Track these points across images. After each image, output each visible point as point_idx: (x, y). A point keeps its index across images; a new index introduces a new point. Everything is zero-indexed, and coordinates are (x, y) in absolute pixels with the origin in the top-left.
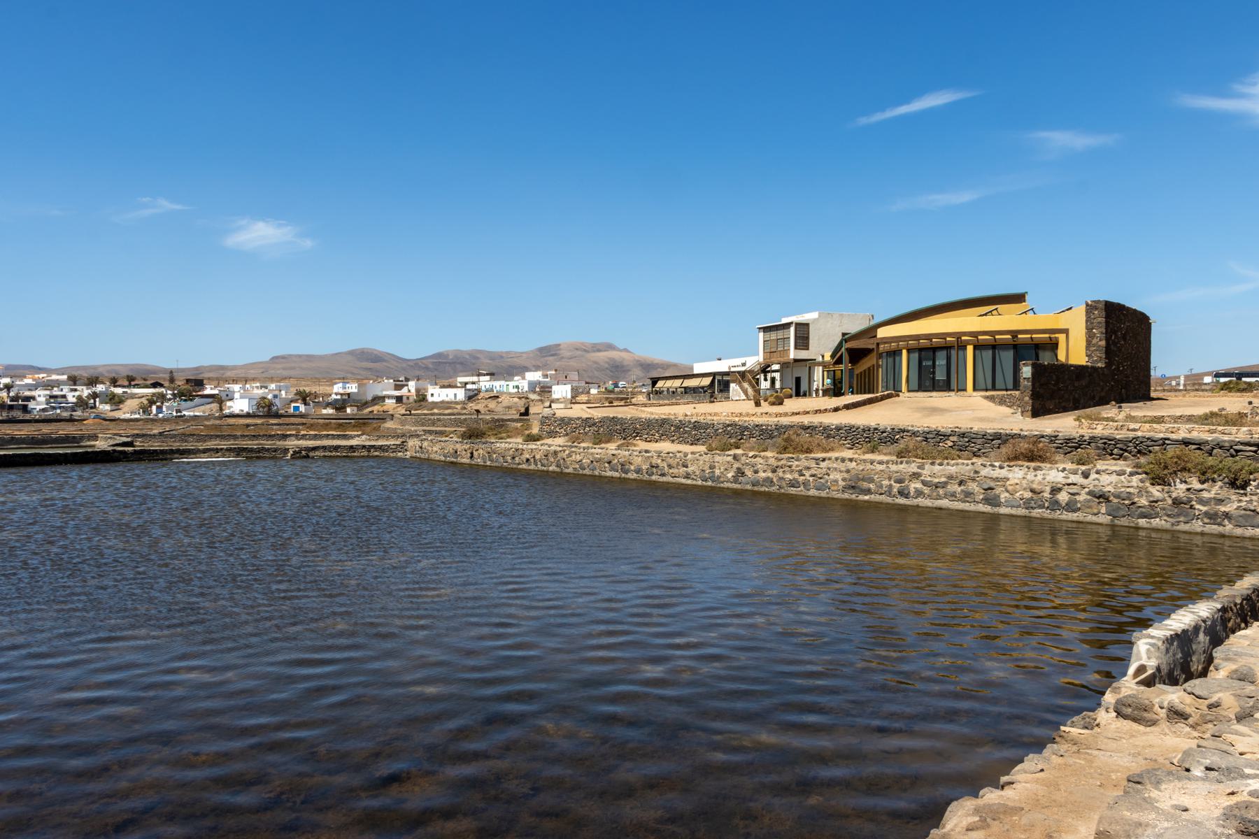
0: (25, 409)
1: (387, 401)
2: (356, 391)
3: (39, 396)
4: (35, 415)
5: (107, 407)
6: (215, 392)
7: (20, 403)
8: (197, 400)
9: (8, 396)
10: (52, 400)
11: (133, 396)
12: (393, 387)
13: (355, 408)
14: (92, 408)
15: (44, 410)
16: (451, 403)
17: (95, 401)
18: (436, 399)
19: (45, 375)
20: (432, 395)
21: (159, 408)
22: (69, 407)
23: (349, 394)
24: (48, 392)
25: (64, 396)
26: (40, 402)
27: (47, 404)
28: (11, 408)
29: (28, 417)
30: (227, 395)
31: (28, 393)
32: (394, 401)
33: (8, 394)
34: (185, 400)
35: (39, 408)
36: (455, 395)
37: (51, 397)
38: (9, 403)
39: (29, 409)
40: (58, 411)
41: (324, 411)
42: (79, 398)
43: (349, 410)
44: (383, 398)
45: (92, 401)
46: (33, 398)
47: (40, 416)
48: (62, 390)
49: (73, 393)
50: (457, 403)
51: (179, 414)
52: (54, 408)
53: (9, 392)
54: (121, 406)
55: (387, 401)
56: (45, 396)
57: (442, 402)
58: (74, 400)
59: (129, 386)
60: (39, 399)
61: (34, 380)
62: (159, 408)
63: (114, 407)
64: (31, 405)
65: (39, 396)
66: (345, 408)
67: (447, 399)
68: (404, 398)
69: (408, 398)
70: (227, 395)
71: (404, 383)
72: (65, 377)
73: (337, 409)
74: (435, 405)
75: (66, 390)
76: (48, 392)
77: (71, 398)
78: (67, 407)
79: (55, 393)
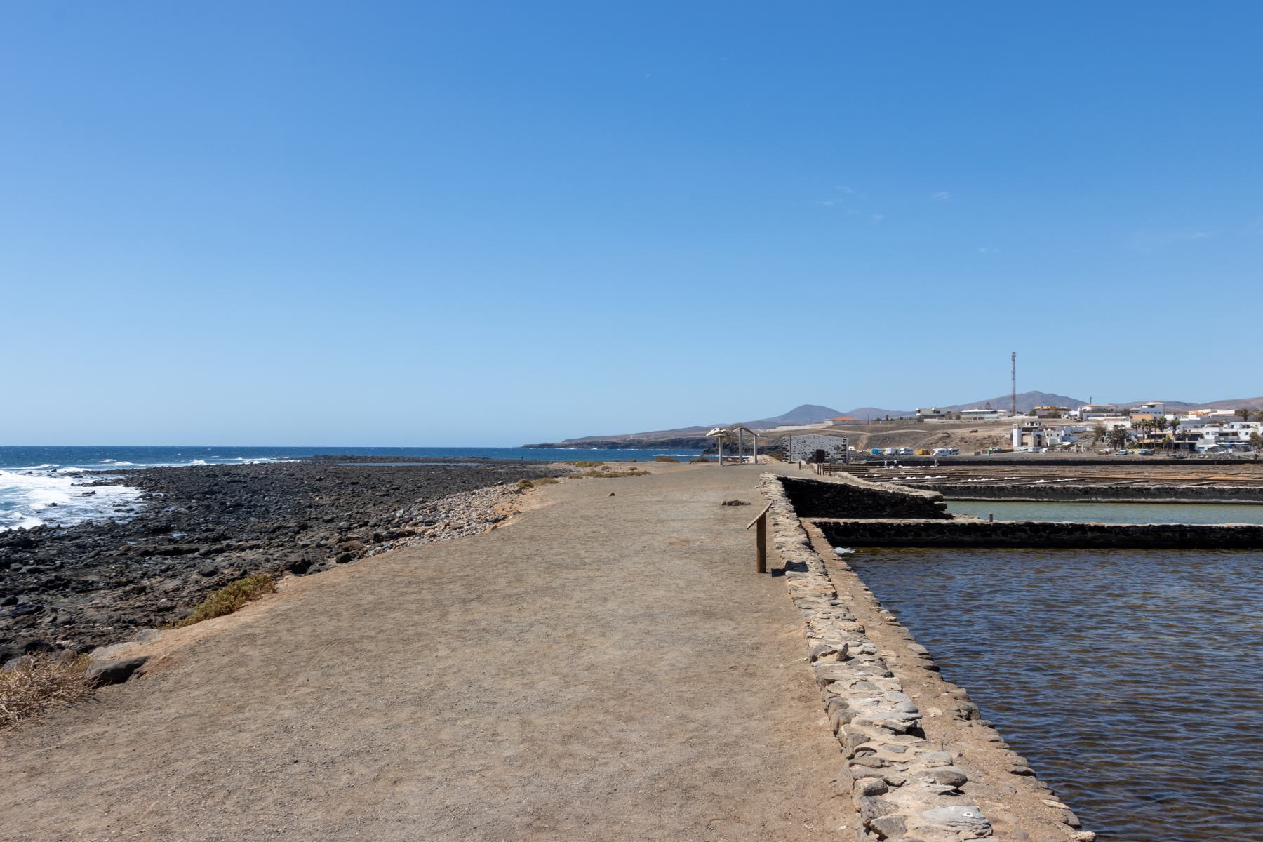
0: (1192, 448)
3: (1207, 433)
4: (1204, 454)
7: (1187, 441)
9: (1174, 434)
10: (1222, 439)
15: (1212, 449)
19: (1209, 411)
22: (1242, 446)
24: (1217, 430)
25: (1235, 434)
26: (1208, 440)
27: (1216, 443)
28: (1177, 446)
29: (1196, 457)
31: (1194, 431)
33: (1174, 432)
35: (1207, 447)
37: (1221, 434)
38: (1175, 442)
39: (1196, 449)
40: (1230, 451)
42: (1254, 435)
46: (1201, 436)
47: (1210, 456)
48: (1232, 427)
52: (1224, 447)
53: (1175, 428)
56: (1214, 433)
58: (1247, 438)
60: (1207, 437)
61: (1198, 416)
64: (1199, 443)
65: (1207, 433)
72: (1232, 412)
75: (1237, 426)
76: (1217, 430)
77: (1244, 436)
78: (1239, 446)
79: (1225, 430)
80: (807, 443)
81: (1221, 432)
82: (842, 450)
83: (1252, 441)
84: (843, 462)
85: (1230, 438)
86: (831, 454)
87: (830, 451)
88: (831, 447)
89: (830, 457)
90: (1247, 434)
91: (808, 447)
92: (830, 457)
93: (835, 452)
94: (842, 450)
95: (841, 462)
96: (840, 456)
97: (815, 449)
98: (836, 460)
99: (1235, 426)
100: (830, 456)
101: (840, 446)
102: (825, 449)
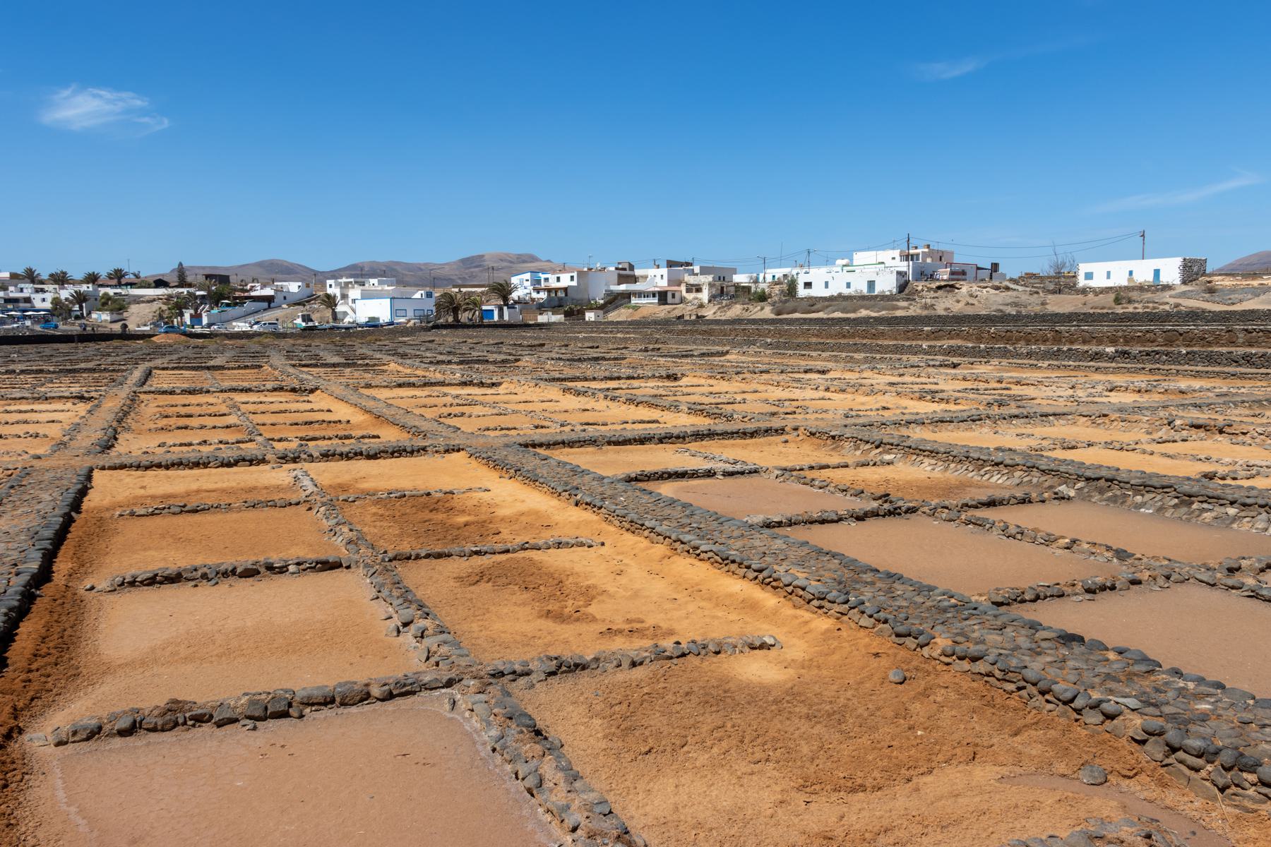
1: (634, 301)
2: (574, 283)
5: (106, 316)
6: (268, 292)
8: (248, 304)
10: (10, 306)
11: (138, 300)
12: (615, 278)
13: (600, 312)
14: (77, 318)
16: (863, 298)
17: (81, 308)
18: (818, 291)
20: (808, 285)
21: (196, 318)
23: (566, 290)
25: (28, 300)
30: (285, 298)
32: (656, 300)
34: (228, 305)
36: (1157, 272)
40: (28, 323)
41: (542, 319)
42: (56, 302)
43: (590, 316)
44: (627, 296)
45: (77, 307)
48: (22, 290)
49: (41, 296)
50: (883, 297)
51: (310, 324)
54: (125, 314)
55: (634, 301)
57: (840, 297)
58: (48, 305)
59: (120, 285)
62: (196, 318)
63: (116, 317)
66: (581, 313)
67: (846, 292)
68: (669, 295)
69: (673, 296)
70: (285, 298)
71: (628, 272)
73: (568, 314)
74: (813, 303)
77: (43, 302)
78: (35, 317)
81: (7, 297)
83: (56, 309)
85: (22, 305)
90: (44, 300)
99: (25, 290)
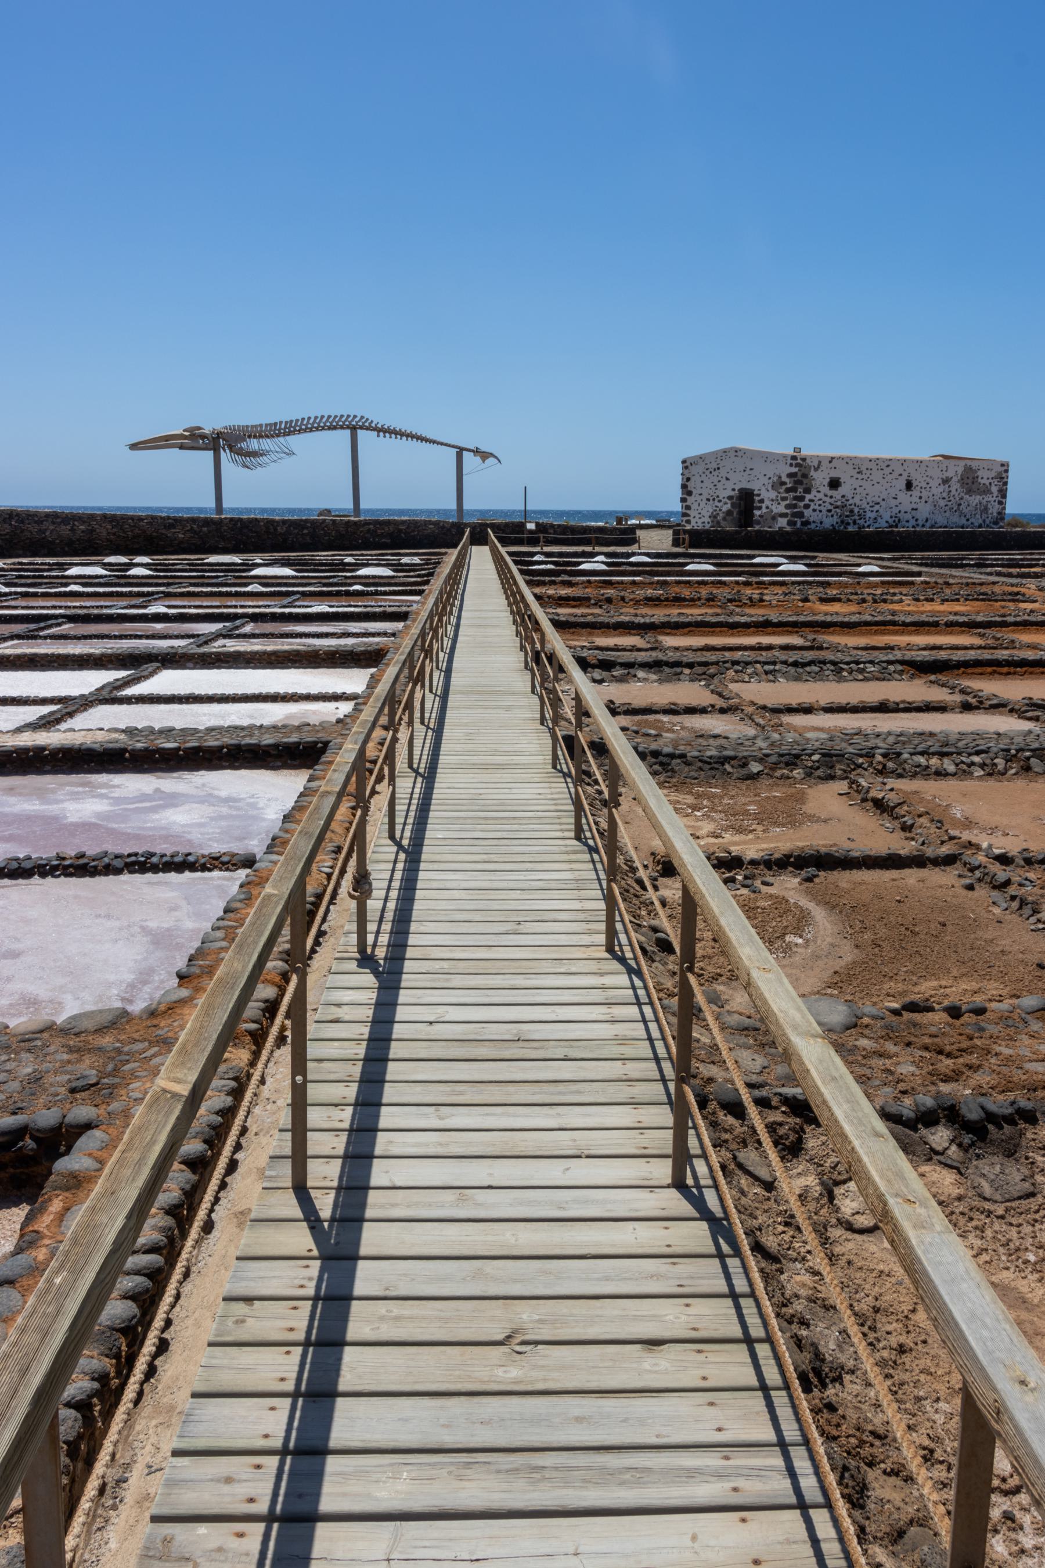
80: (723, 473)
82: (788, 490)
84: (789, 523)
86: (767, 502)
87: (765, 495)
88: (765, 480)
89: (764, 510)
91: (724, 481)
92: (764, 510)
93: (773, 494)
94: (788, 490)
95: (782, 522)
96: (781, 509)
97: (737, 488)
98: (774, 518)
100: (764, 506)
101: (784, 479)
102: (755, 486)
